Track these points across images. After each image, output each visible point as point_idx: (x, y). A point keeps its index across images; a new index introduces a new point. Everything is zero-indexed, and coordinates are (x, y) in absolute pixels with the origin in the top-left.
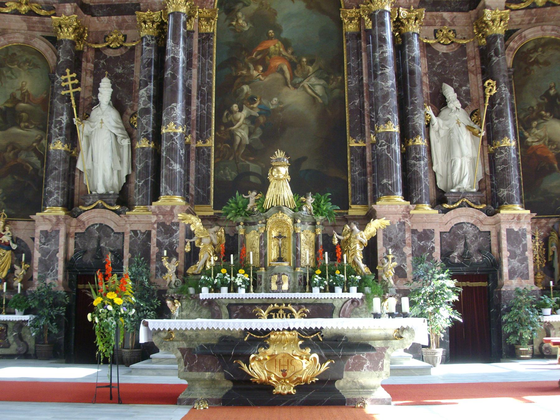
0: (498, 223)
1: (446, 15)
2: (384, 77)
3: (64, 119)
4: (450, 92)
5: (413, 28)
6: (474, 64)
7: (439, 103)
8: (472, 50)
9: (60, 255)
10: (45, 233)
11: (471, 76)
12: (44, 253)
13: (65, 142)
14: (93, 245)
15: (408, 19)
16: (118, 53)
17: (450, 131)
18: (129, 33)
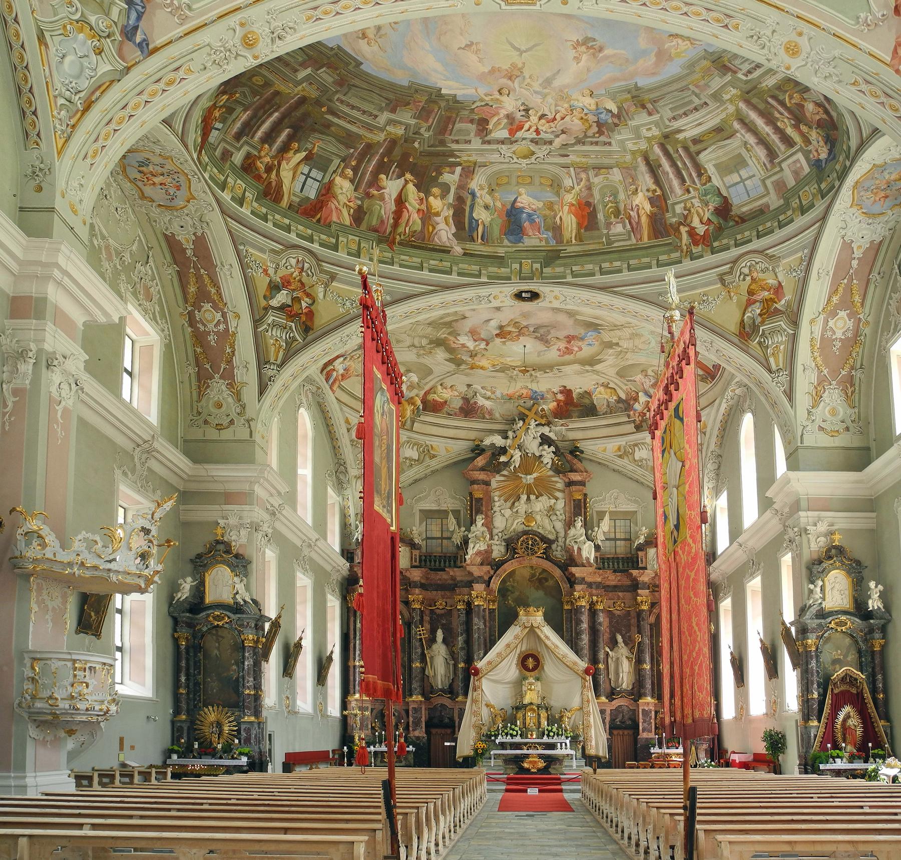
0: (638, 706)
1: (620, 594)
2: (581, 640)
3: (419, 650)
4: (619, 638)
5: (600, 607)
6: (634, 621)
7: (613, 644)
8: (633, 614)
9: (423, 719)
10: (414, 708)
11: (632, 628)
12: (415, 718)
13: (421, 663)
14: (438, 714)
15: (597, 602)
16: (443, 612)
17: (618, 659)
18: (448, 600)
